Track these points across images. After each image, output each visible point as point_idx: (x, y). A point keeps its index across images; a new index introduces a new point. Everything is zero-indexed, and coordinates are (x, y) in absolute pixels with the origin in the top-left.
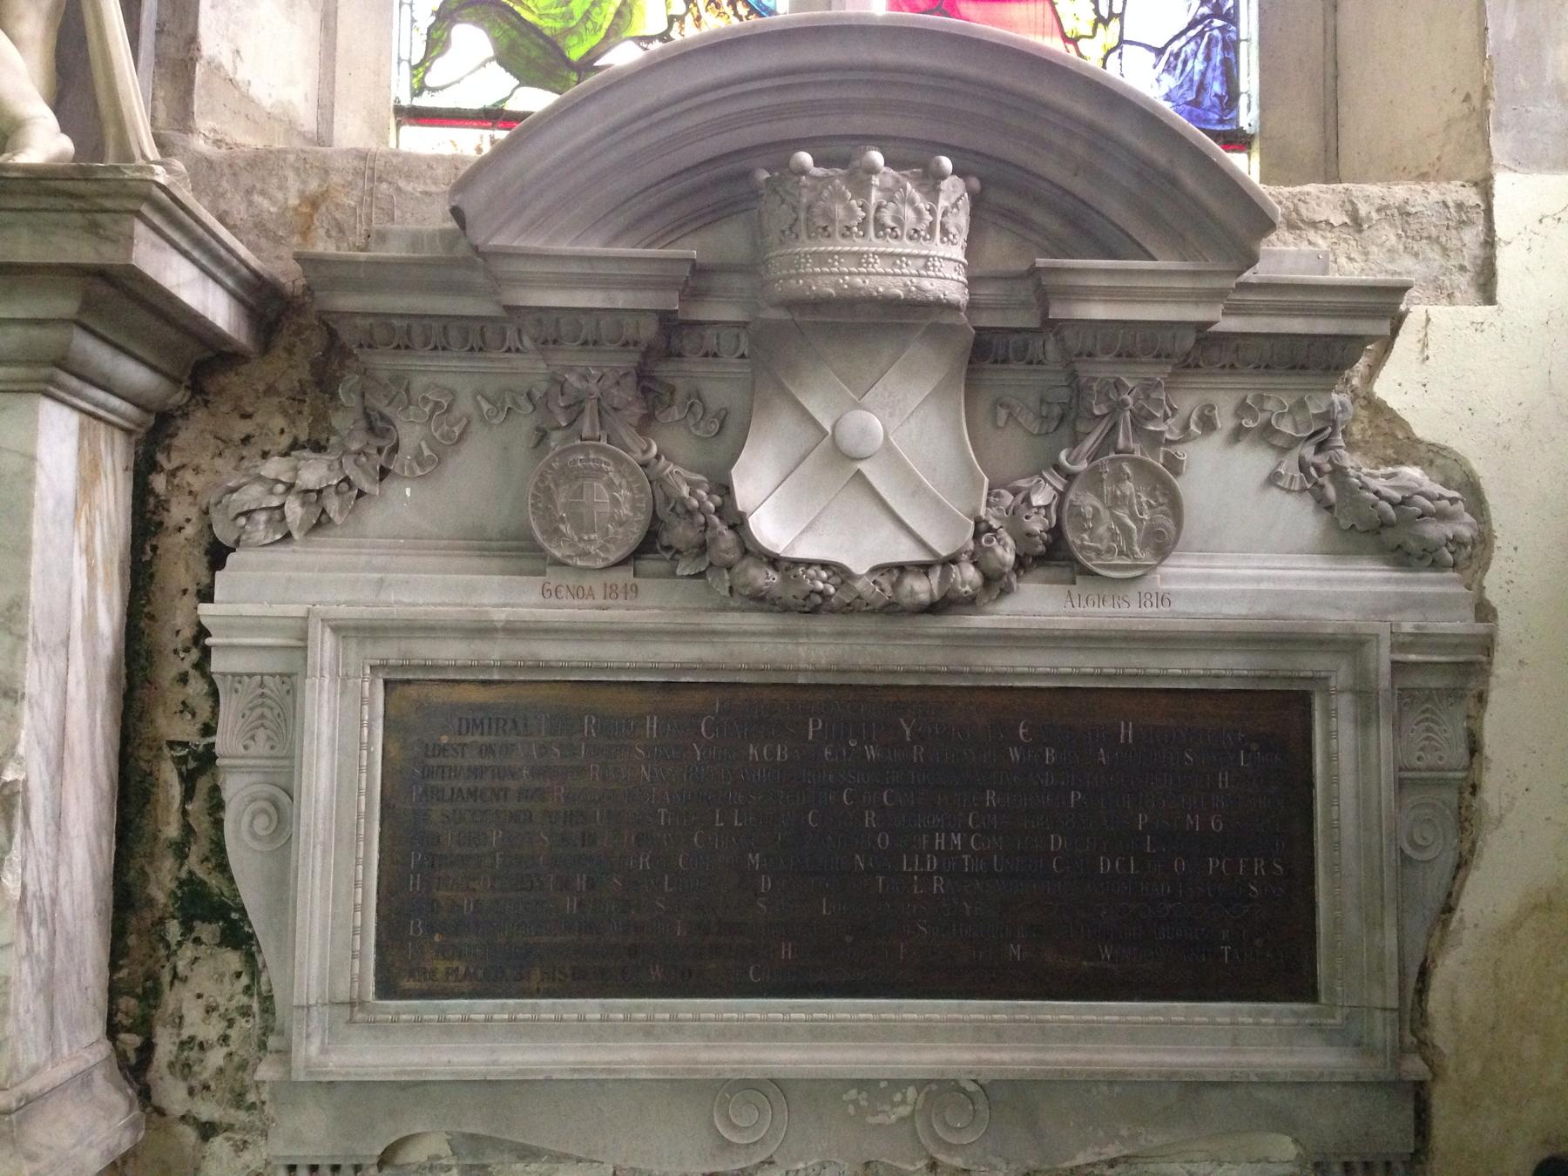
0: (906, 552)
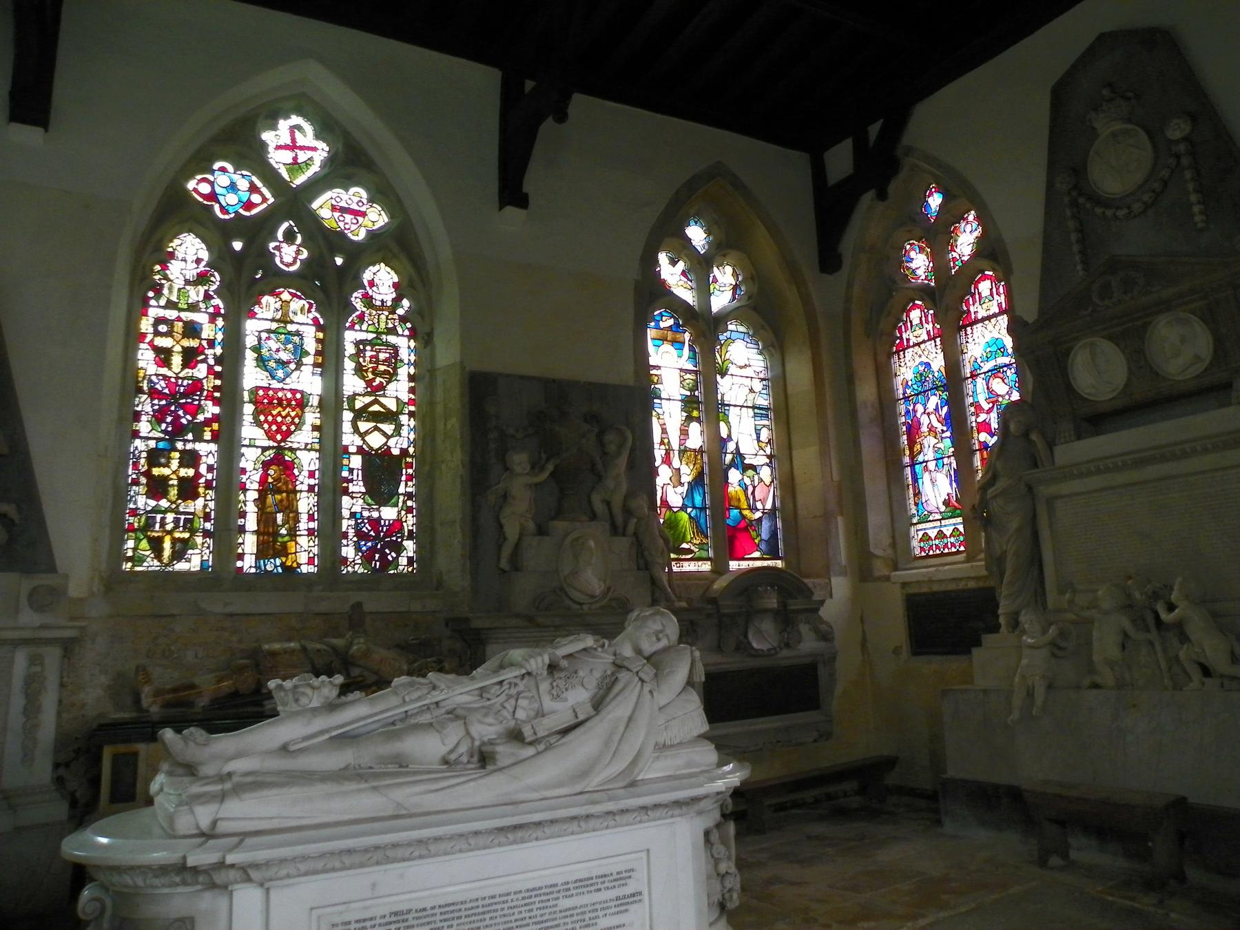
0: (770, 647)
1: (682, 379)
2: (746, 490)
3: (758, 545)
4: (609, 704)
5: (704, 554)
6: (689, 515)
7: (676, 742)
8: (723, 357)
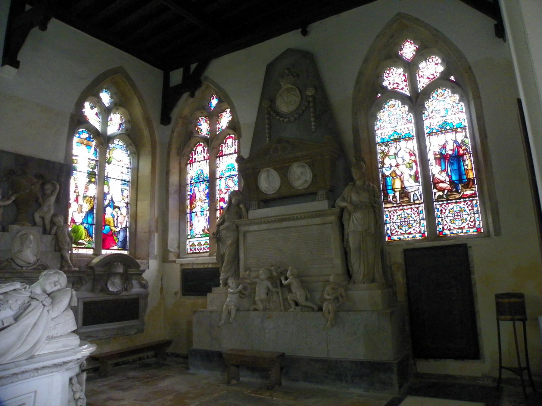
1: (89, 163)
2: (114, 217)
3: (117, 243)
4: (24, 317)
5: (90, 246)
6: (85, 227)
7: (59, 335)
8: (110, 155)
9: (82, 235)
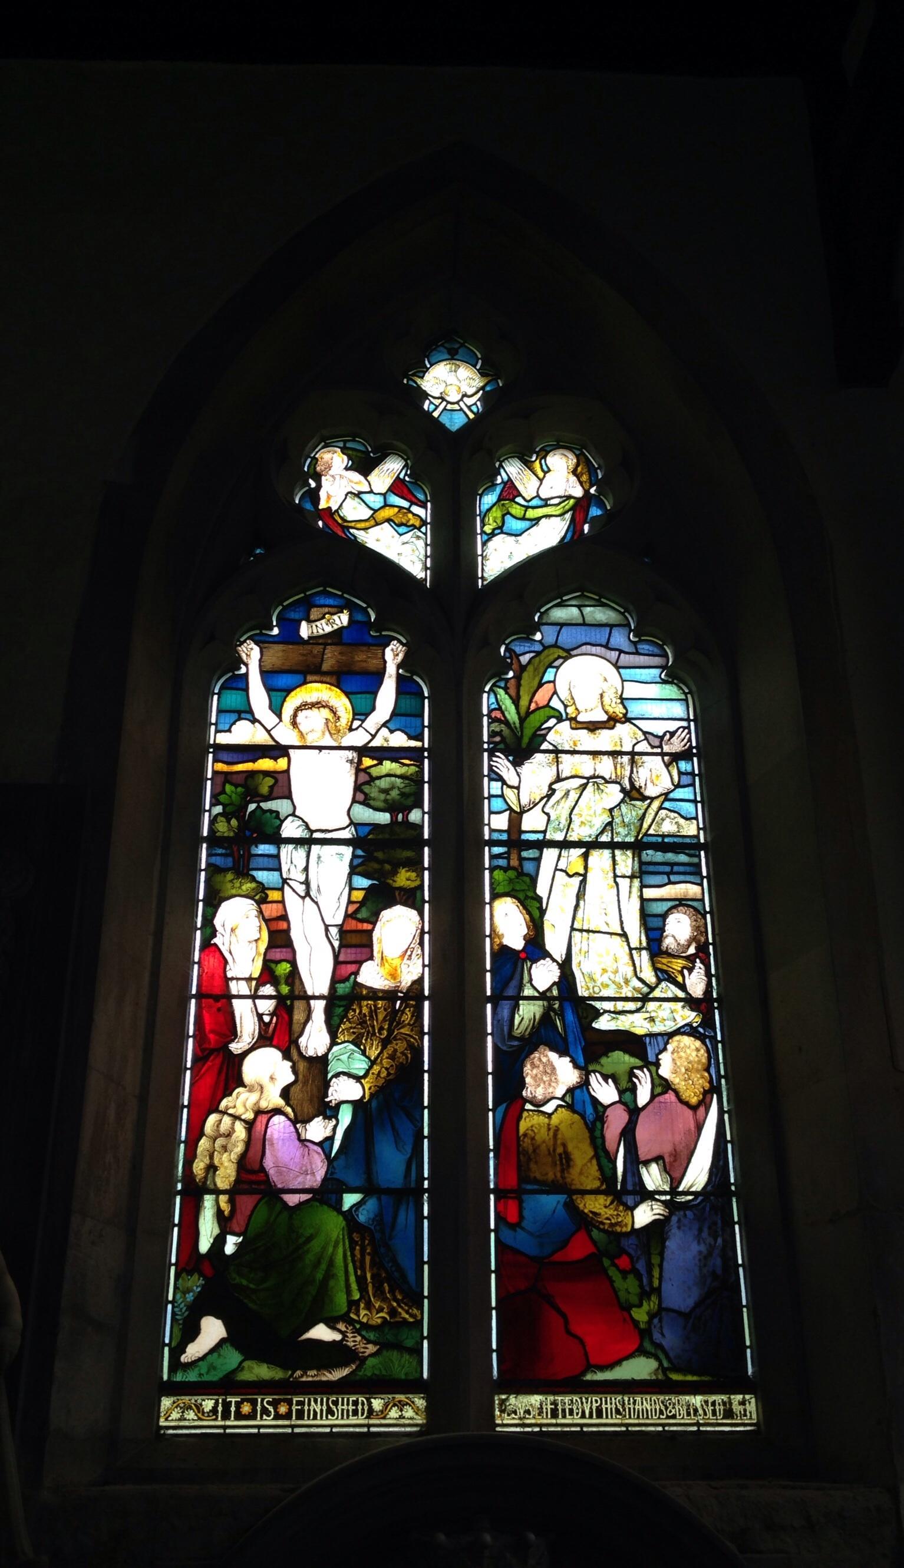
1: (363, 777)
8: (524, 702)
9: (332, 1283)
